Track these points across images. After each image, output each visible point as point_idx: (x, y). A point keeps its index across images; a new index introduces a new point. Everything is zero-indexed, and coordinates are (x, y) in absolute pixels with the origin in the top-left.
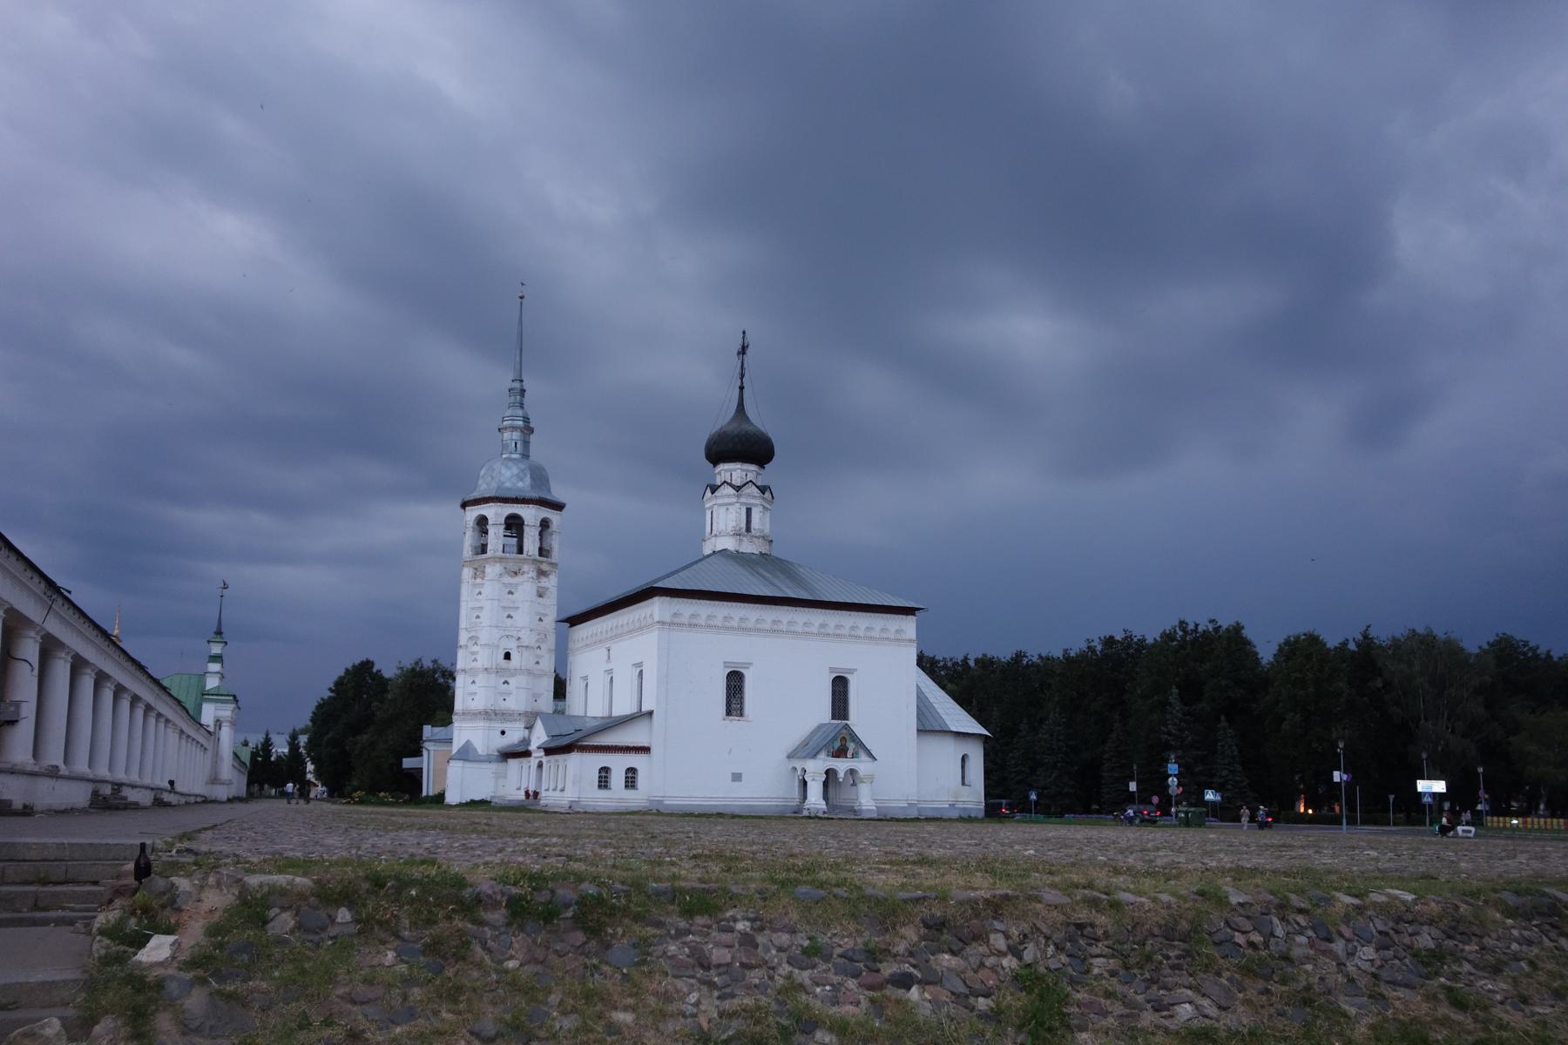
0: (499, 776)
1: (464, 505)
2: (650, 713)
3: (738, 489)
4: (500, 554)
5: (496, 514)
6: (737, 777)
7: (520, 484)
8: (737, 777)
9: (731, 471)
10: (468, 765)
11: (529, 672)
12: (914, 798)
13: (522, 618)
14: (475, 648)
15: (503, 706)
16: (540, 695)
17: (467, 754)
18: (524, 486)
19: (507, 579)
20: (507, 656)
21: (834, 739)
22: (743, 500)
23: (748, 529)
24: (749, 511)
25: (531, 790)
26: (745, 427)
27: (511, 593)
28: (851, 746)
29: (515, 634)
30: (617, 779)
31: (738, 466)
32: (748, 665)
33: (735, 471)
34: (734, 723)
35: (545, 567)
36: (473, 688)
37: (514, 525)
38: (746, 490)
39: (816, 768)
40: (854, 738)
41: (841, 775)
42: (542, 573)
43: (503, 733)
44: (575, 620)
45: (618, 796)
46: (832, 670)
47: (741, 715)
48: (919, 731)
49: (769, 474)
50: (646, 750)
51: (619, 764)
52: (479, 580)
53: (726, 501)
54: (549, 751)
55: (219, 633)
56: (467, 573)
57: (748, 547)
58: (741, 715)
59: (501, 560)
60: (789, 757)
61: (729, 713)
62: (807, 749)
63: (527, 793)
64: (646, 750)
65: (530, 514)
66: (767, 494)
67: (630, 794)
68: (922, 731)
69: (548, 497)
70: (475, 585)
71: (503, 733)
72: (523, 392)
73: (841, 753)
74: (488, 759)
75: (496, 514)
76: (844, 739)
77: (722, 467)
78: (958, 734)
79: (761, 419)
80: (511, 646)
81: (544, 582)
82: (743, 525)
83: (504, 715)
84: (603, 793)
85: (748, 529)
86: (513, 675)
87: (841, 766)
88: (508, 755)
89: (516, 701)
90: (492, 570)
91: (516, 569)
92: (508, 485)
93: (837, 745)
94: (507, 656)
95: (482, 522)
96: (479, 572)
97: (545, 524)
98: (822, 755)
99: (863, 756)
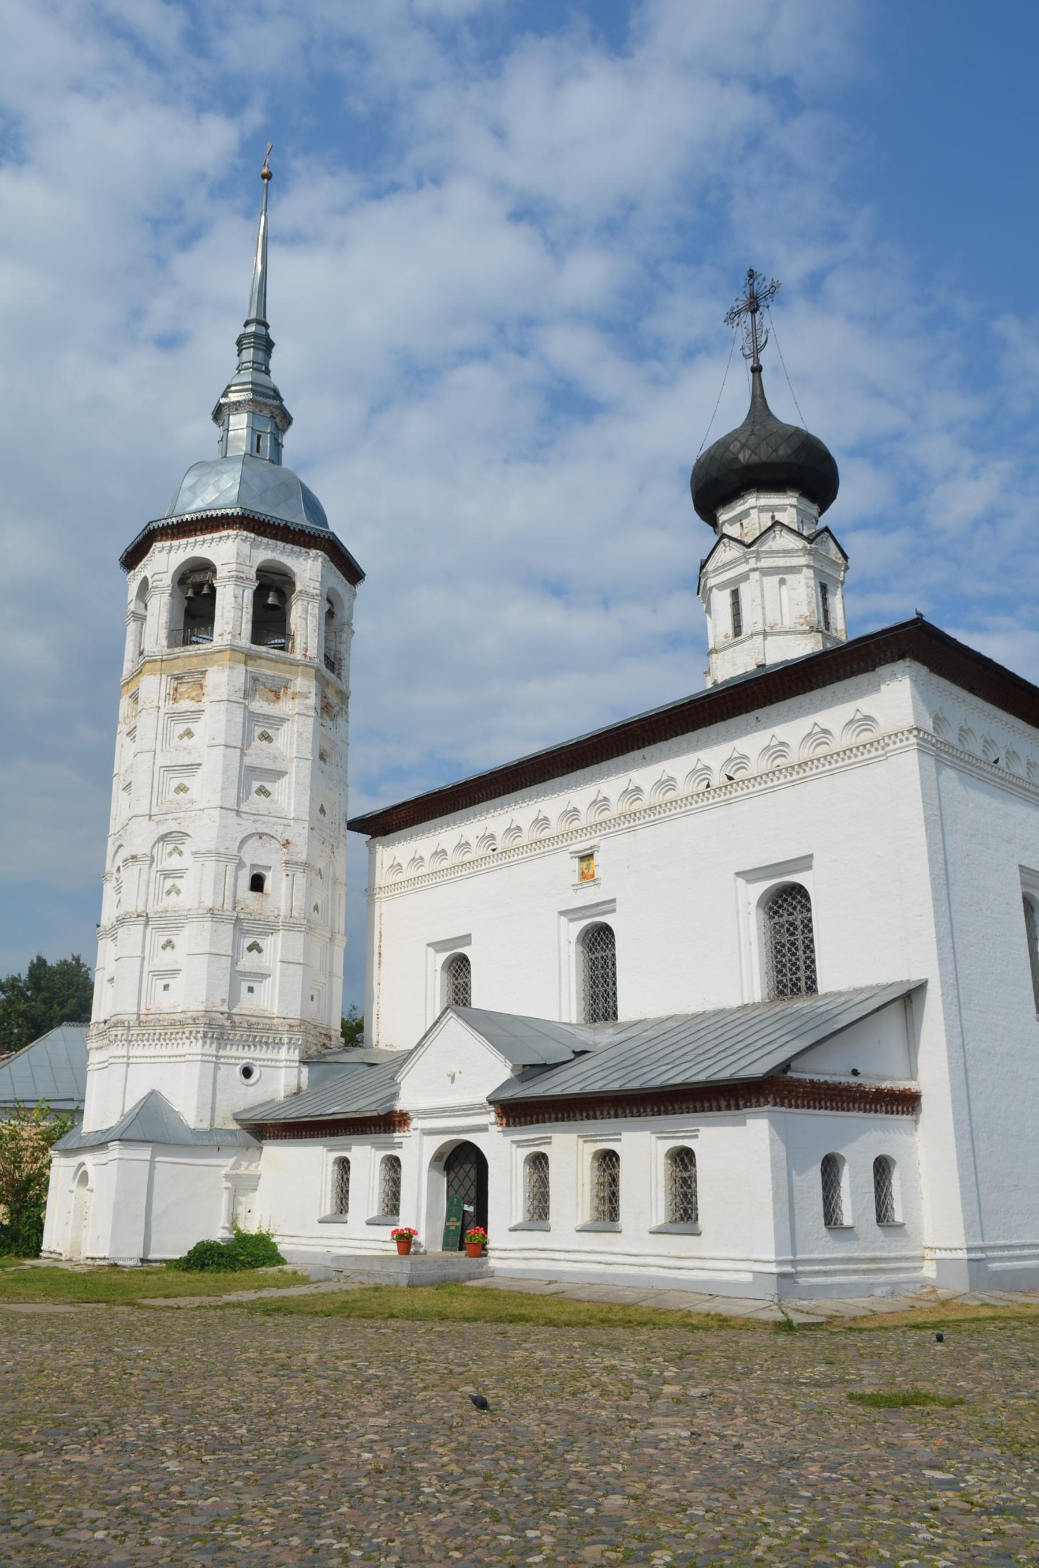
0: (241, 1186)
1: (133, 558)
3: (810, 540)
13: (291, 796)
15: (247, 1004)
17: (149, 1128)
24: (824, 588)
29: (277, 831)
31: (789, 499)
33: (786, 506)
36: (165, 959)
43: (247, 1072)
44: (380, 825)
50: (905, 1102)
52: (185, 705)
53: (781, 562)
54: (514, 1111)
56: (153, 687)
63: (405, 1240)
64: (905, 1102)
70: (175, 716)
71: (247, 1072)
72: (265, 345)
74: (205, 1142)
83: (258, 1032)
86: (270, 929)
88: (265, 1130)
89: (274, 998)
94: (257, 883)
96: (187, 681)
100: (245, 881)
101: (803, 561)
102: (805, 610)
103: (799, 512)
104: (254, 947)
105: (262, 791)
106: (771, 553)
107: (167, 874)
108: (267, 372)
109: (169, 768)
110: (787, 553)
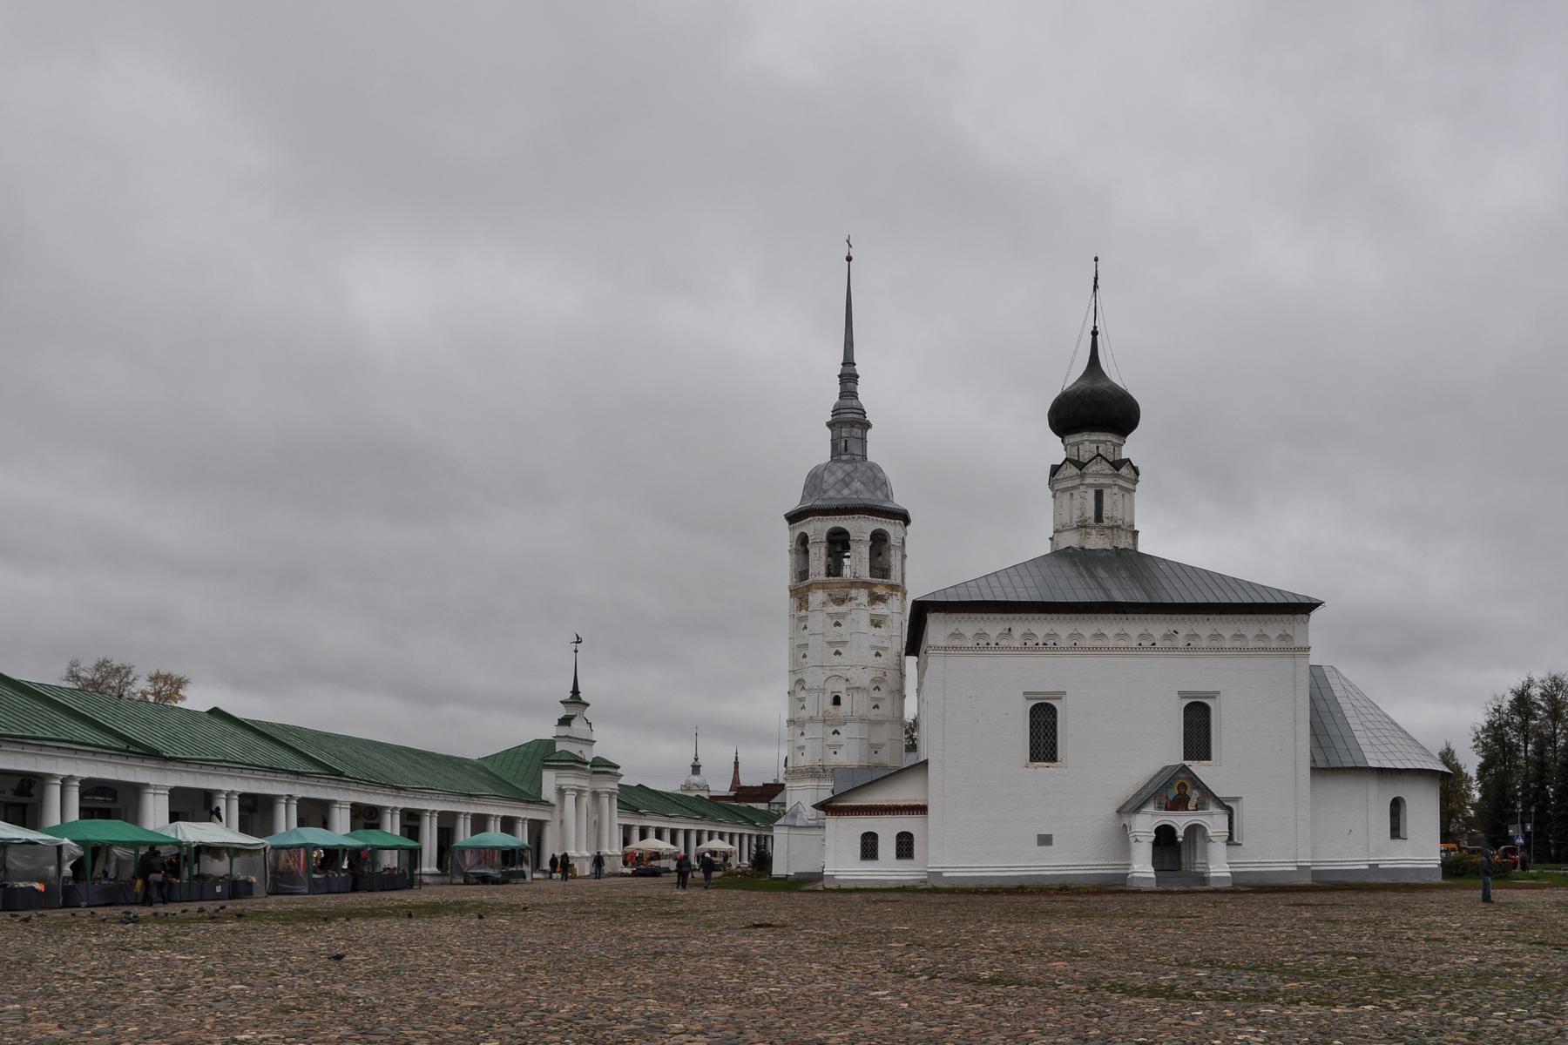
2: (926, 762)
3: (1080, 465)
4: (822, 577)
5: (817, 529)
6: (1045, 840)
7: (846, 492)
8: (1045, 840)
9: (1077, 444)
10: (793, 831)
11: (862, 720)
12: (1305, 859)
14: (803, 694)
16: (881, 746)
18: (857, 492)
19: (833, 608)
20: (837, 701)
21: (1167, 785)
22: (1089, 481)
23: (1099, 517)
25: (558, 854)
26: (1101, 385)
27: (837, 624)
28: (1194, 795)
30: (887, 847)
31: (1085, 436)
32: (1060, 695)
34: (1042, 769)
35: (880, 591)
37: (839, 543)
38: (1092, 468)
39: (1146, 824)
40: (1198, 784)
41: (1180, 833)
42: (875, 599)
45: (888, 869)
46: (1182, 695)
47: (1054, 760)
48: (1316, 771)
49: (1132, 447)
50: (922, 809)
51: (887, 829)
52: (803, 612)
53: (1069, 484)
55: (575, 692)
57: (1096, 542)
58: (1054, 760)
59: (823, 586)
60: (1119, 812)
61: (1036, 756)
62: (1134, 806)
64: (922, 809)
65: (860, 528)
66: (1124, 471)
67: (905, 865)
68: (1323, 770)
69: (888, 505)
70: (801, 619)
73: (1179, 804)
75: (817, 529)
76: (1183, 786)
77: (1071, 439)
78: (1382, 773)
79: (1119, 373)
80: (840, 687)
81: (880, 609)
82: (1091, 513)
84: (869, 865)
85: (1099, 517)
87: (1180, 822)
90: (816, 597)
91: (842, 594)
92: (832, 493)
93: (1173, 793)
94: (837, 701)
95: (803, 540)
97: (879, 539)
98: (1150, 808)
99: (1213, 809)
100: (829, 699)
101: (1077, 482)
102: (1077, 513)
103: (1092, 442)
104: (836, 732)
105: (838, 653)
106: (1064, 479)
107: (802, 700)
108: (854, 395)
109: (799, 646)
110: (1071, 478)
